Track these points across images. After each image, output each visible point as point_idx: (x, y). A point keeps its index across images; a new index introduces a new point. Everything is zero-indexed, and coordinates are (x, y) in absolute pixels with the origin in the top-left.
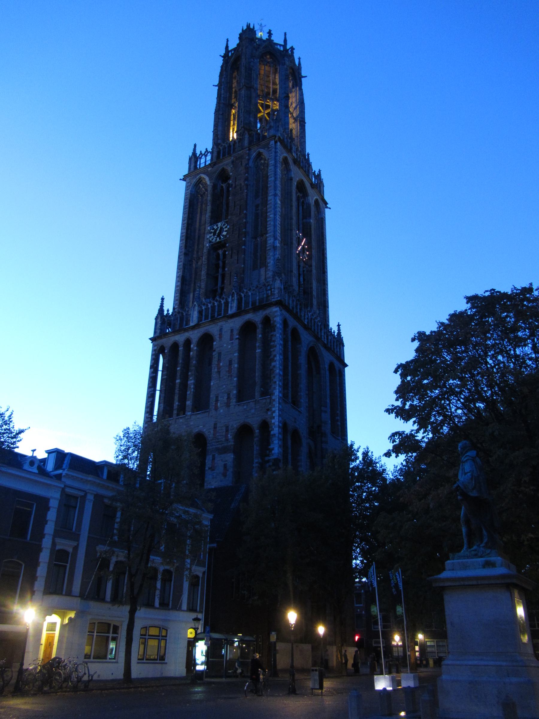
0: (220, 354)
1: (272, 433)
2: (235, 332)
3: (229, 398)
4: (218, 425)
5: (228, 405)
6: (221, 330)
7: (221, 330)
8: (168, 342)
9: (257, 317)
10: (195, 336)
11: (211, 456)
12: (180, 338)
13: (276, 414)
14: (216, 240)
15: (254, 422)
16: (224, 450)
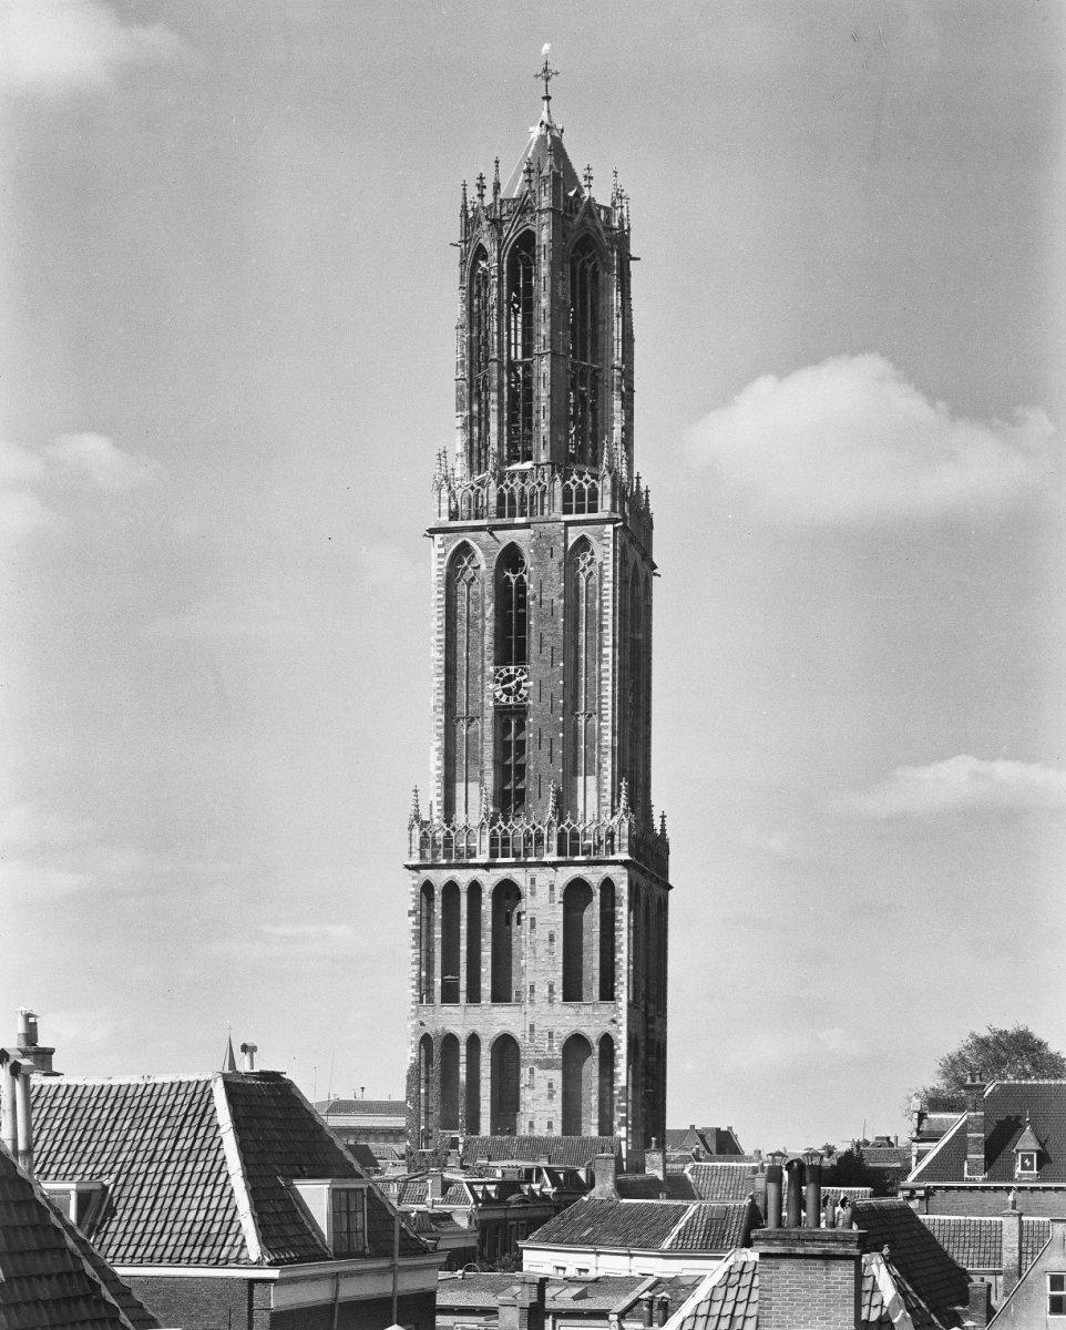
0: (533, 920)
1: (618, 1052)
2: (558, 894)
3: (551, 990)
4: (536, 1028)
5: (551, 1001)
6: (533, 881)
7: (533, 881)
8: (440, 878)
9: (594, 876)
10: (489, 880)
11: (528, 1070)
12: (463, 878)
13: (624, 1029)
14: (508, 700)
15: (593, 1034)
16: (547, 1065)
